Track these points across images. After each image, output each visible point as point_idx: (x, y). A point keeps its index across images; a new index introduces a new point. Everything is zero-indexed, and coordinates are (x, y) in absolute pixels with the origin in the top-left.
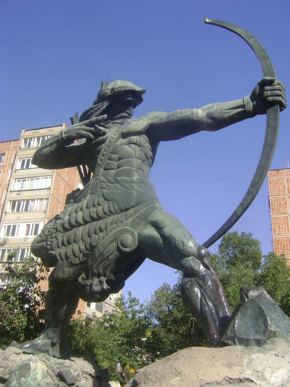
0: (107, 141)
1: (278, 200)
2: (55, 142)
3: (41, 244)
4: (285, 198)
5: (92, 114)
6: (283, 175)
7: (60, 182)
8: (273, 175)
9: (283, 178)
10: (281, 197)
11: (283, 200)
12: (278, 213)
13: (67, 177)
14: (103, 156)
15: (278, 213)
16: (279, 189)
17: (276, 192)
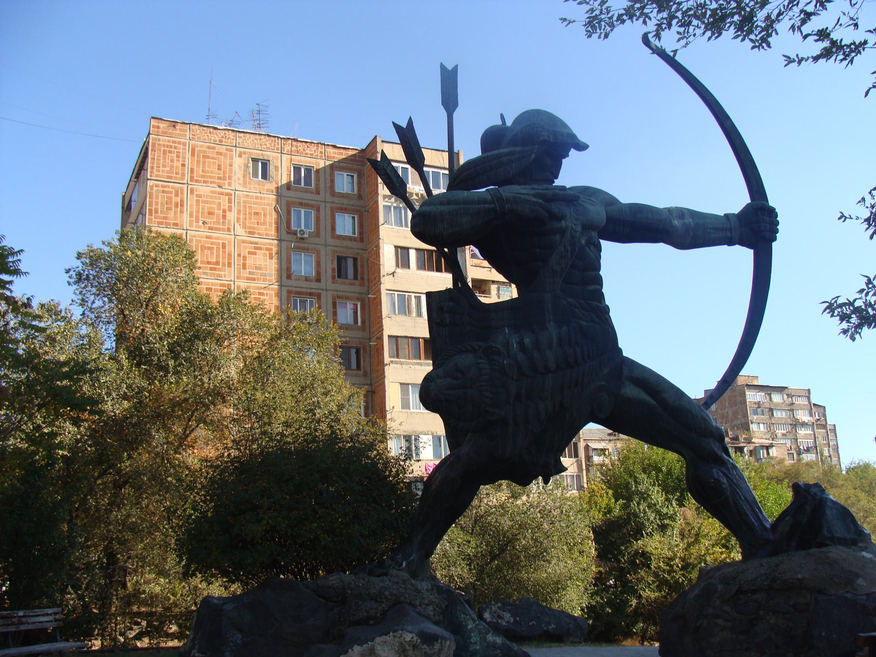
1: (167, 192)
4: (182, 190)
6: (186, 135)
8: (162, 132)
10: (173, 188)
11: (177, 195)
12: (162, 223)
15: (159, 223)
16: (172, 167)
17: (163, 172)
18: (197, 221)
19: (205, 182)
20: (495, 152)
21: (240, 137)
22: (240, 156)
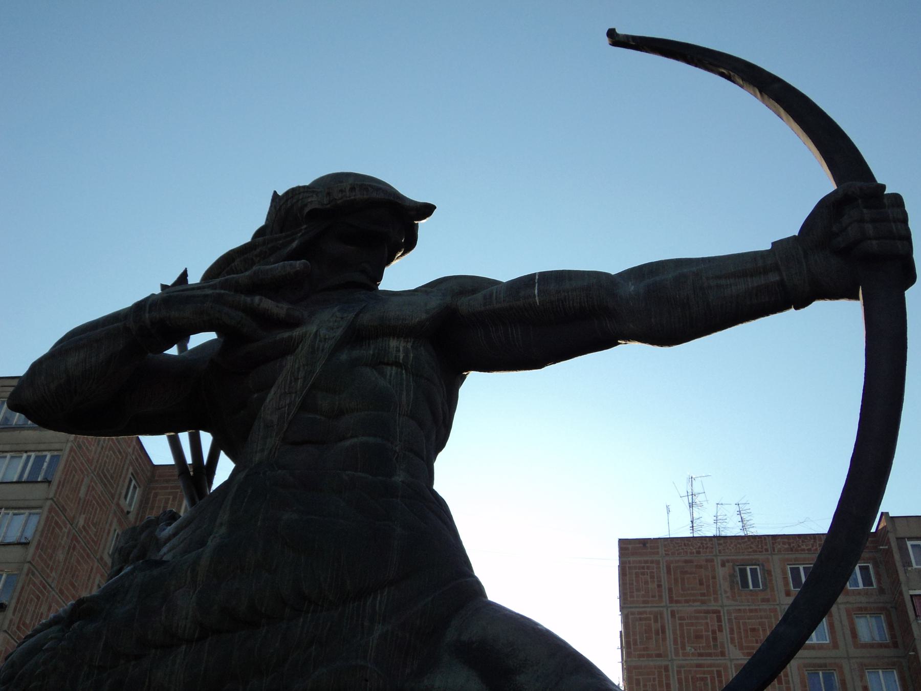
1: (646, 619)
4: (661, 614)
6: (658, 553)
7: (61, 528)
9: (658, 563)
11: (656, 621)
12: (643, 656)
13: (83, 516)
18: (683, 648)
19: (687, 601)
21: (719, 544)
22: (723, 565)
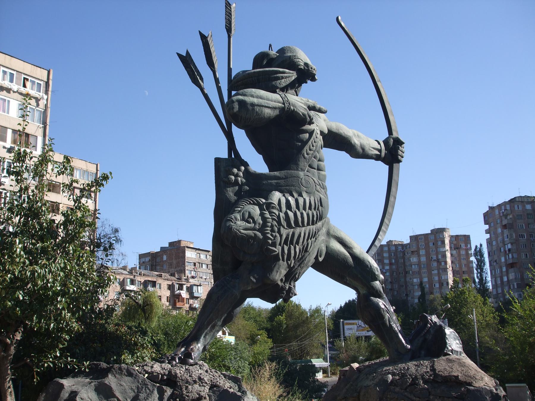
0: (314, 135)
2: (279, 108)
3: (250, 232)
5: (283, 78)
14: (310, 150)
20: (267, 69)
